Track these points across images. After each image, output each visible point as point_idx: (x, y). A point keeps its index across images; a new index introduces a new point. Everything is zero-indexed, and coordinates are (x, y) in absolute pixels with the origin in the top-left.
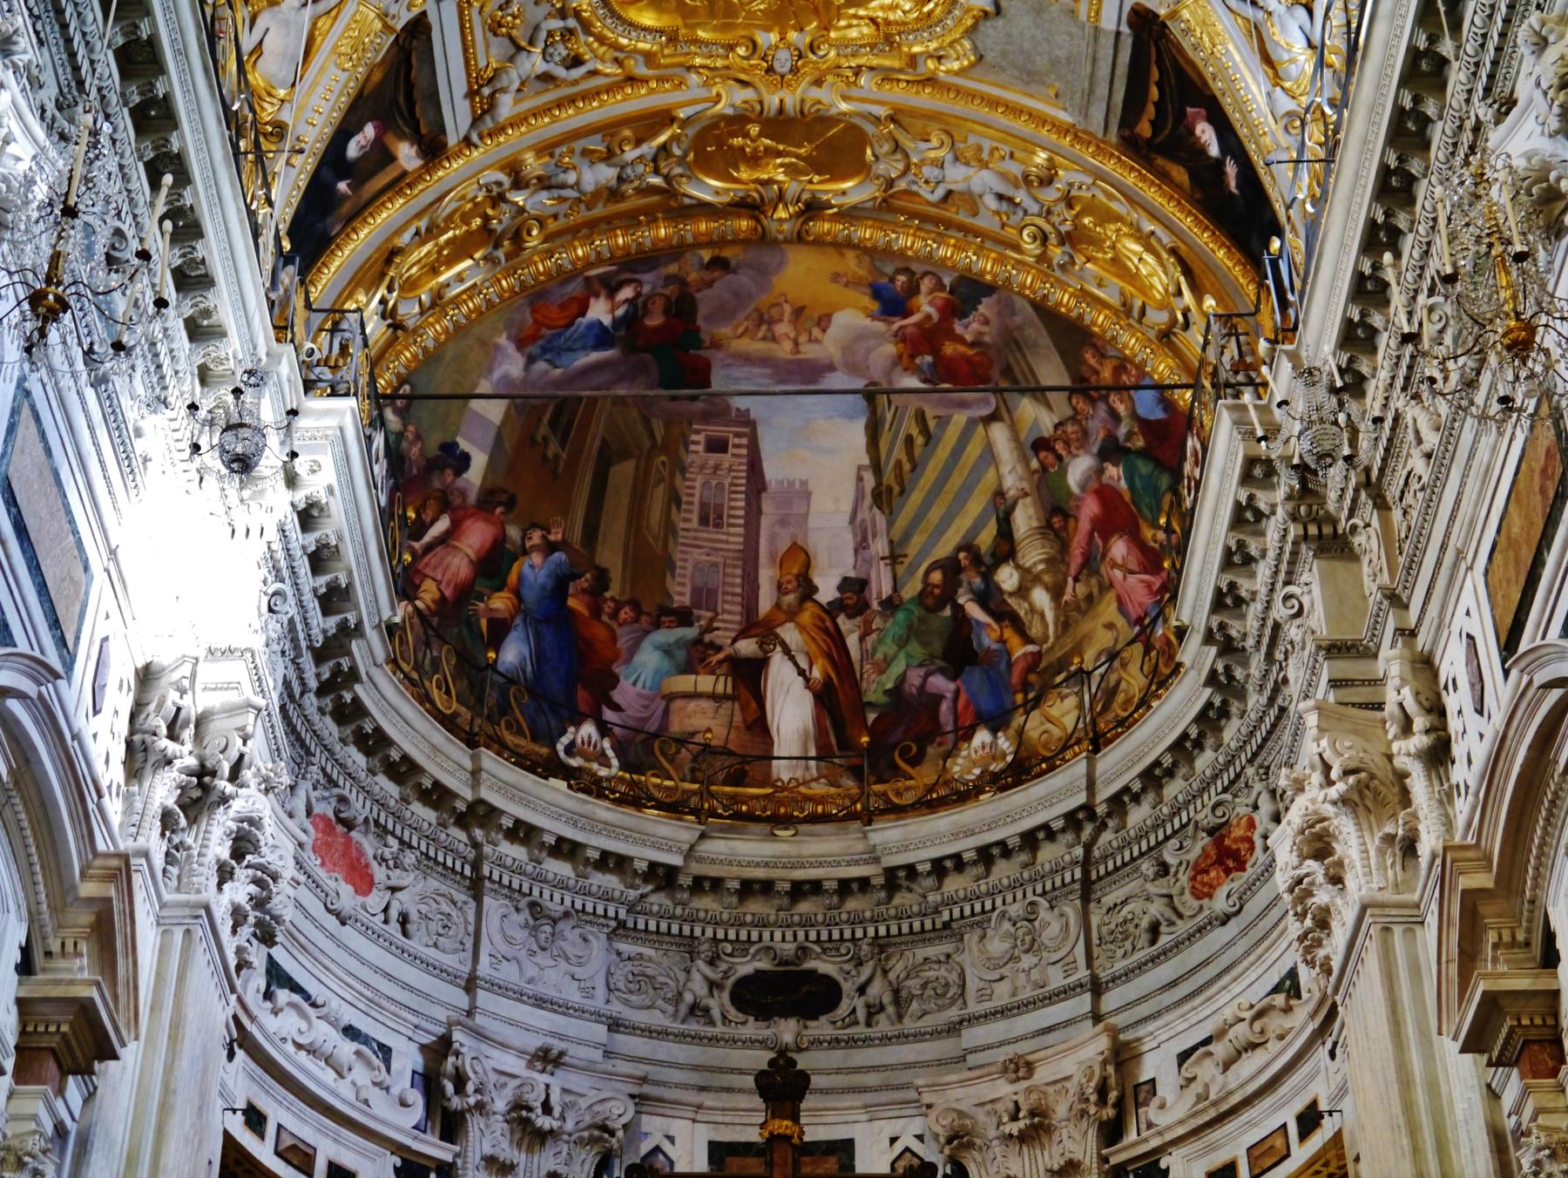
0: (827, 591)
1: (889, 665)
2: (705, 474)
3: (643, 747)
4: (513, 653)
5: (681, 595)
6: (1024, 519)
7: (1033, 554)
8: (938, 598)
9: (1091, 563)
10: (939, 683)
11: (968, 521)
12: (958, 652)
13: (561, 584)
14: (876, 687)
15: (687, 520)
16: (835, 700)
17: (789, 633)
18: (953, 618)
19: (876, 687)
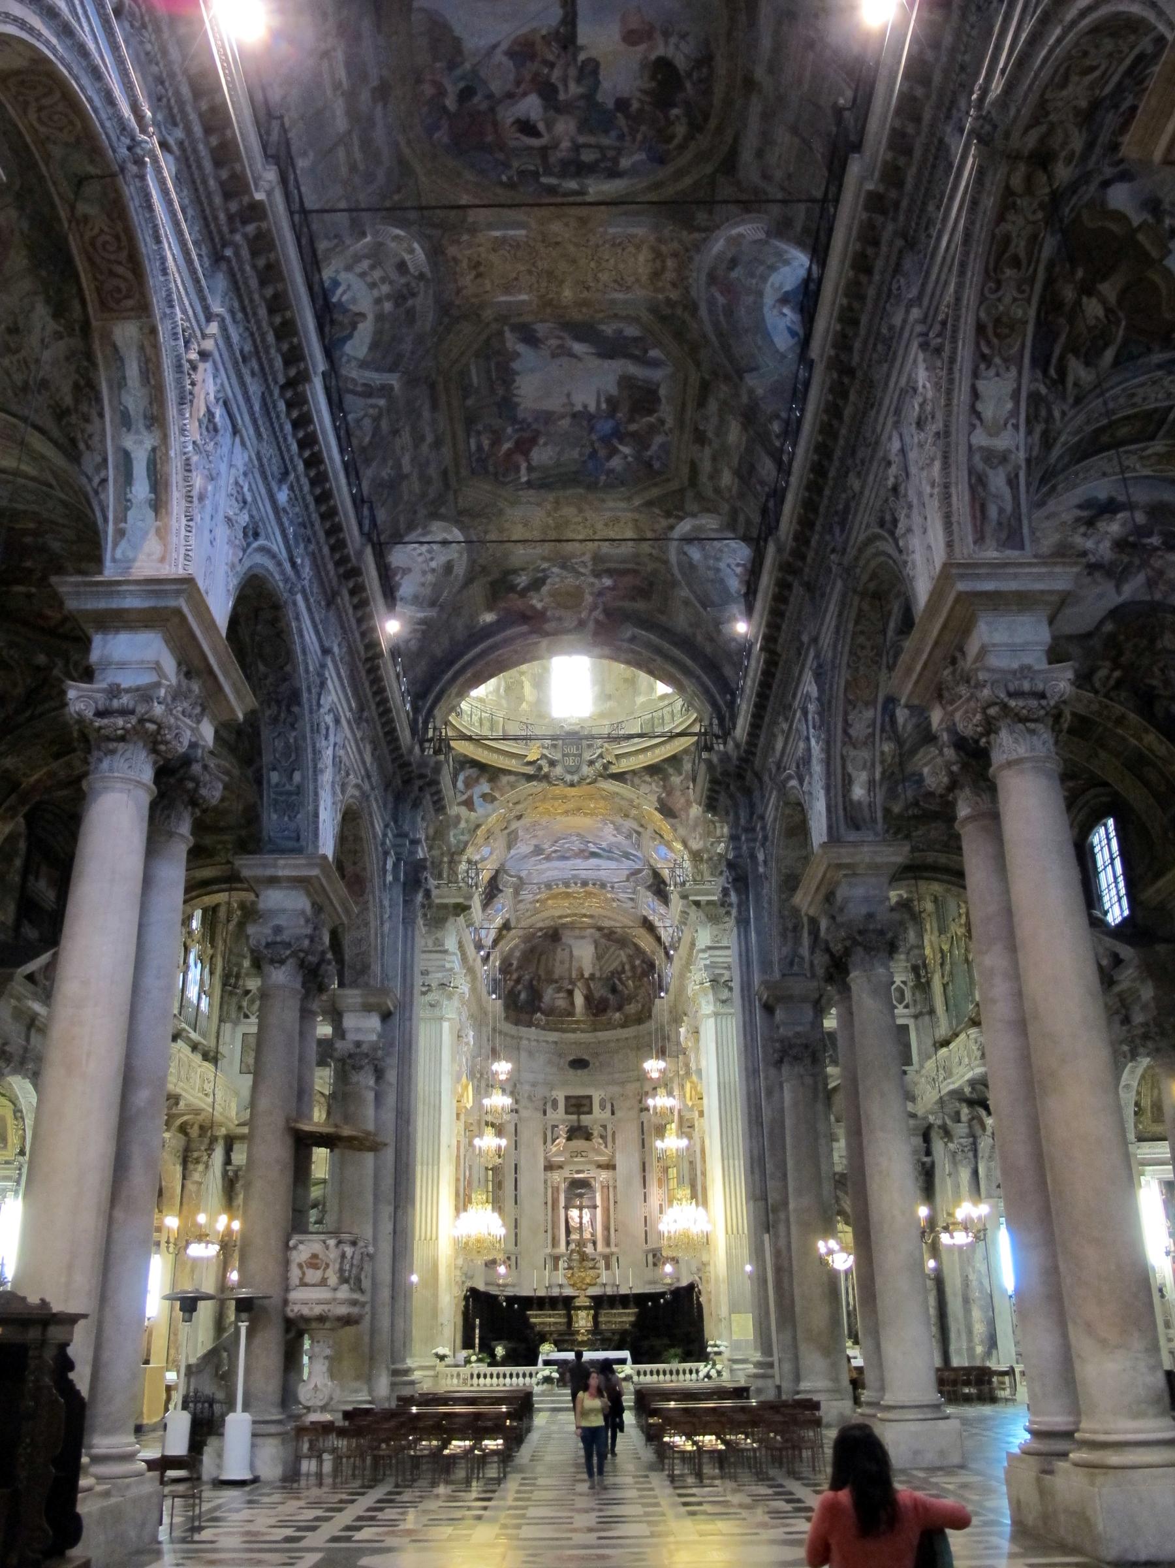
0: (586, 975)
1: (600, 992)
2: (561, 954)
3: (549, 1012)
4: (523, 996)
5: (556, 976)
6: (627, 967)
7: (629, 974)
8: (608, 979)
9: (640, 980)
10: (610, 996)
11: (615, 965)
12: (614, 990)
13: (531, 981)
14: (597, 995)
15: (557, 964)
16: (588, 998)
17: (579, 984)
18: (612, 983)
19: (597, 995)
